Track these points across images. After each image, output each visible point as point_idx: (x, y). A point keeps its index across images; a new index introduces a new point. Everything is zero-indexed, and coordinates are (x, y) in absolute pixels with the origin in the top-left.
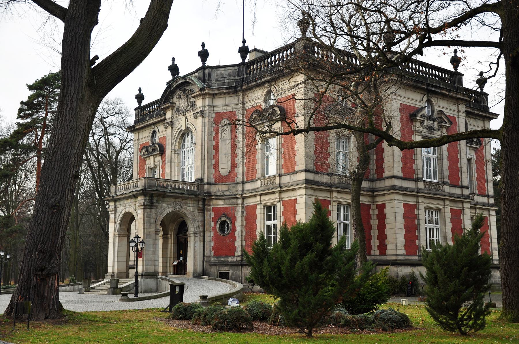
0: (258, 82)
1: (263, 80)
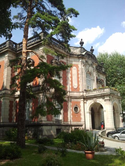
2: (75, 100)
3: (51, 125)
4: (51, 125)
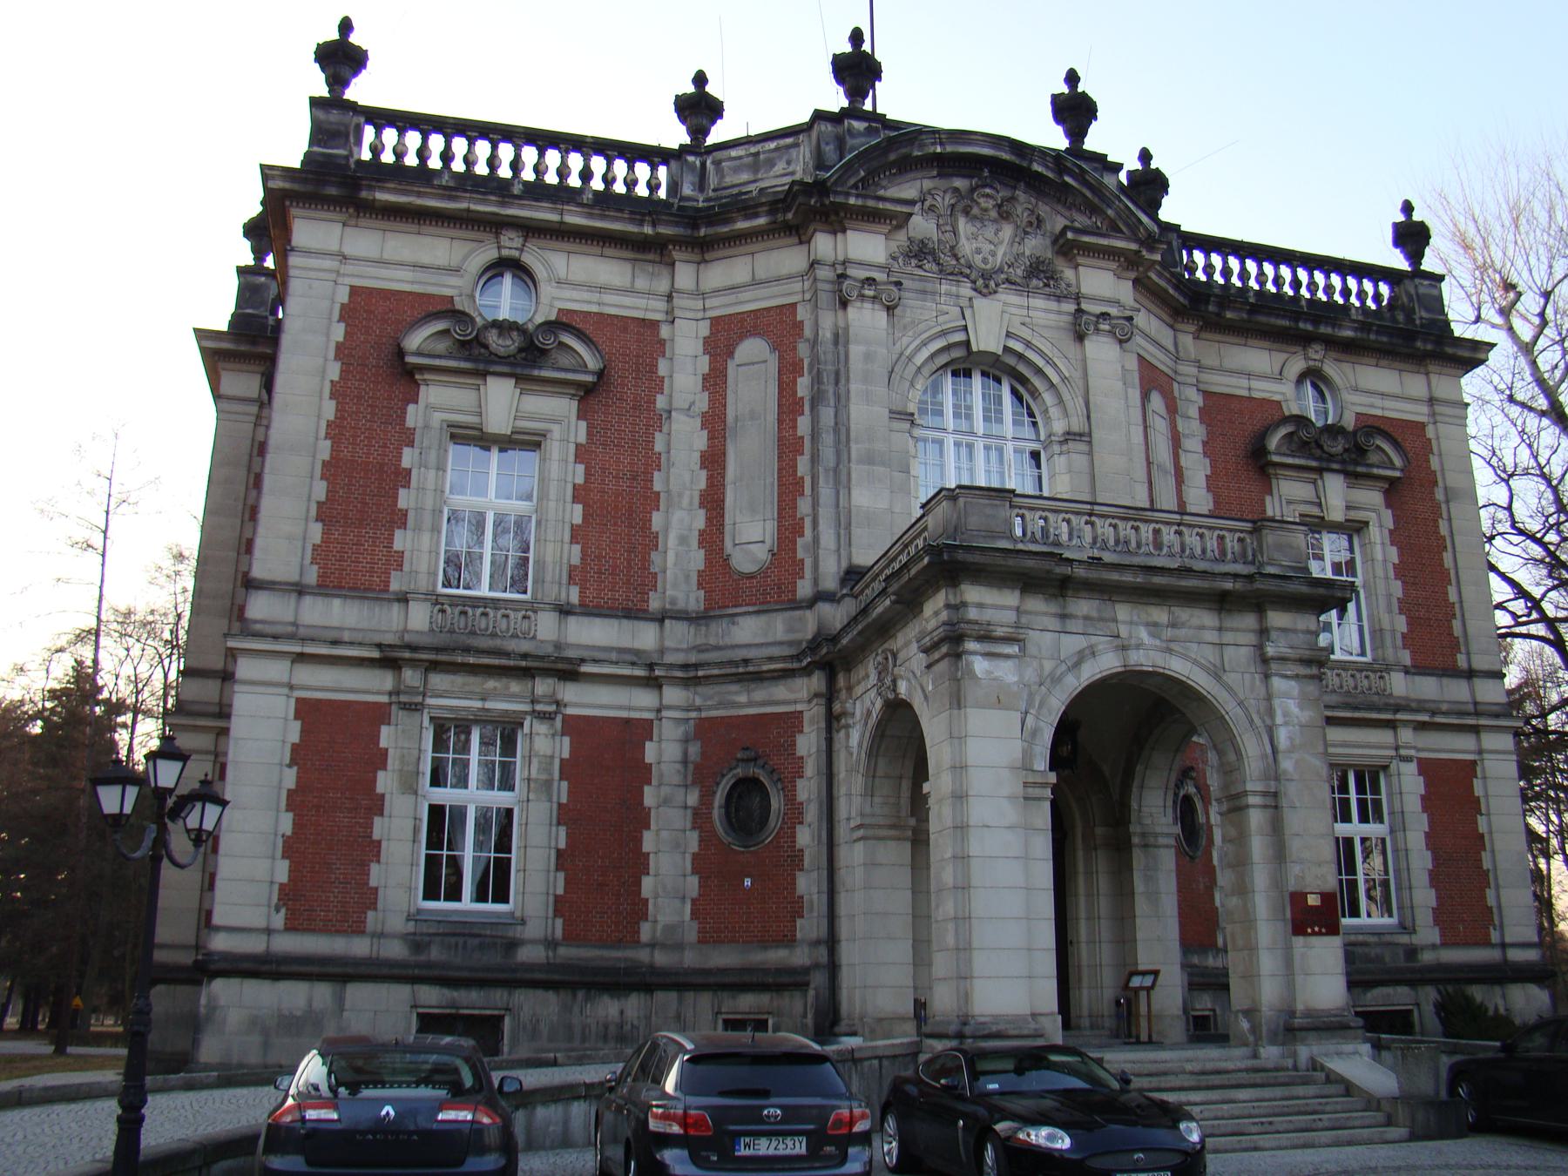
0: (1301, 325)
1: (1323, 329)
2: (743, 699)
3: (340, 973)
4: (340, 973)
